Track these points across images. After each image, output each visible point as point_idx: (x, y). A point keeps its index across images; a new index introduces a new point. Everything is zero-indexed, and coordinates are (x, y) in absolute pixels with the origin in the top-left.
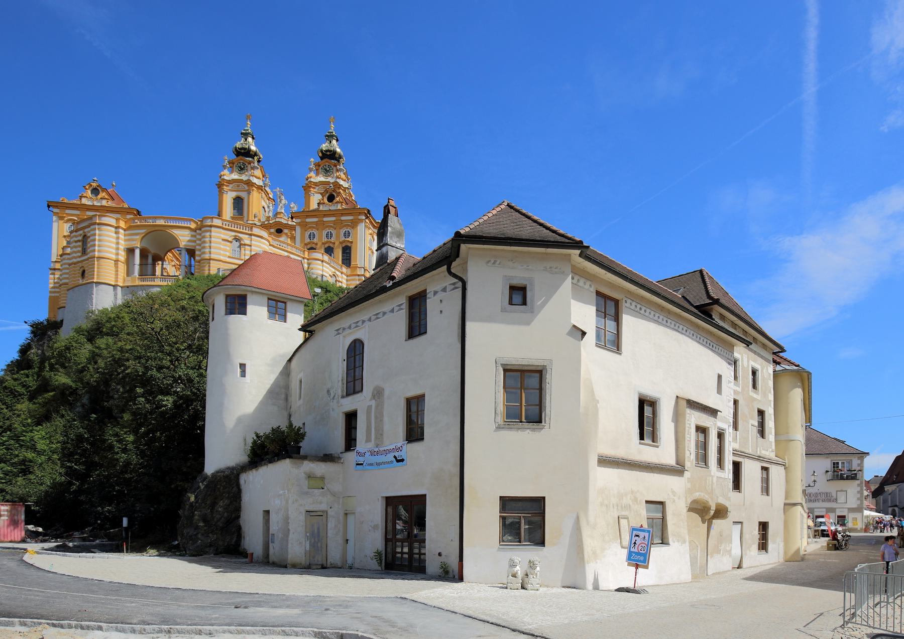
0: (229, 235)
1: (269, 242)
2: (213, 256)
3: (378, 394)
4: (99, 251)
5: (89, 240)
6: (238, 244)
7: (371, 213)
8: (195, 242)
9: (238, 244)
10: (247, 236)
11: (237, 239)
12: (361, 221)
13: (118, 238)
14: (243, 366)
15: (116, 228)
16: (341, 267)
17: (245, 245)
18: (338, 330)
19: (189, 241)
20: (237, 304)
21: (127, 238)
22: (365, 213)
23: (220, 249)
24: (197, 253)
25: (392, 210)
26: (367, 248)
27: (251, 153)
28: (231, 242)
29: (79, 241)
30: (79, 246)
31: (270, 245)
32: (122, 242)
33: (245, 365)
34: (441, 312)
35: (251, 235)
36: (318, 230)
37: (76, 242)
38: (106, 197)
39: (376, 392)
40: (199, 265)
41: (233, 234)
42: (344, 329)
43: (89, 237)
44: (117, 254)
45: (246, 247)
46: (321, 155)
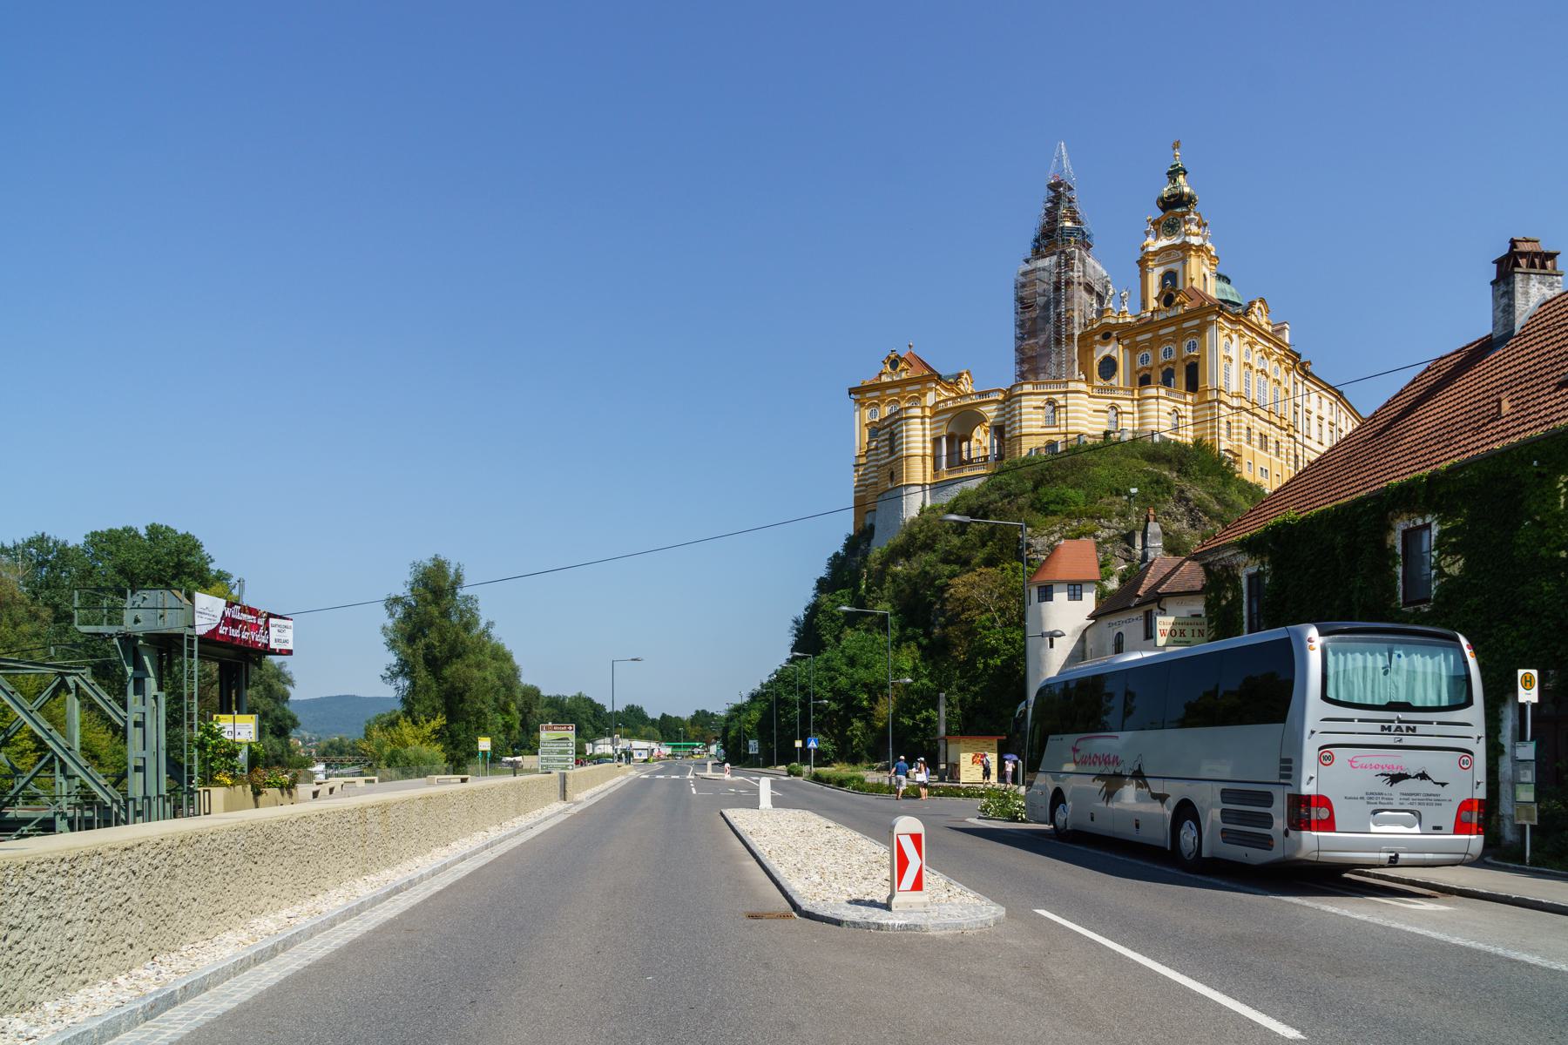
0: (1040, 401)
2: (1024, 431)
4: (907, 449)
6: (1051, 407)
8: (1004, 415)
9: (1051, 407)
11: (1050, 402)
12: (1211, 323)
13: (924, 429)
15: (923, 417)
17: (1060, 407)
19: (997, 416)
20: (1046, 594)
21: (933, 426)
23: (1031, 420)
24: (1007, 429)
28: (1043, 408)
29: (886, 439)
32: (928, 432)
35: (1066, 393)
44: (924, 448)
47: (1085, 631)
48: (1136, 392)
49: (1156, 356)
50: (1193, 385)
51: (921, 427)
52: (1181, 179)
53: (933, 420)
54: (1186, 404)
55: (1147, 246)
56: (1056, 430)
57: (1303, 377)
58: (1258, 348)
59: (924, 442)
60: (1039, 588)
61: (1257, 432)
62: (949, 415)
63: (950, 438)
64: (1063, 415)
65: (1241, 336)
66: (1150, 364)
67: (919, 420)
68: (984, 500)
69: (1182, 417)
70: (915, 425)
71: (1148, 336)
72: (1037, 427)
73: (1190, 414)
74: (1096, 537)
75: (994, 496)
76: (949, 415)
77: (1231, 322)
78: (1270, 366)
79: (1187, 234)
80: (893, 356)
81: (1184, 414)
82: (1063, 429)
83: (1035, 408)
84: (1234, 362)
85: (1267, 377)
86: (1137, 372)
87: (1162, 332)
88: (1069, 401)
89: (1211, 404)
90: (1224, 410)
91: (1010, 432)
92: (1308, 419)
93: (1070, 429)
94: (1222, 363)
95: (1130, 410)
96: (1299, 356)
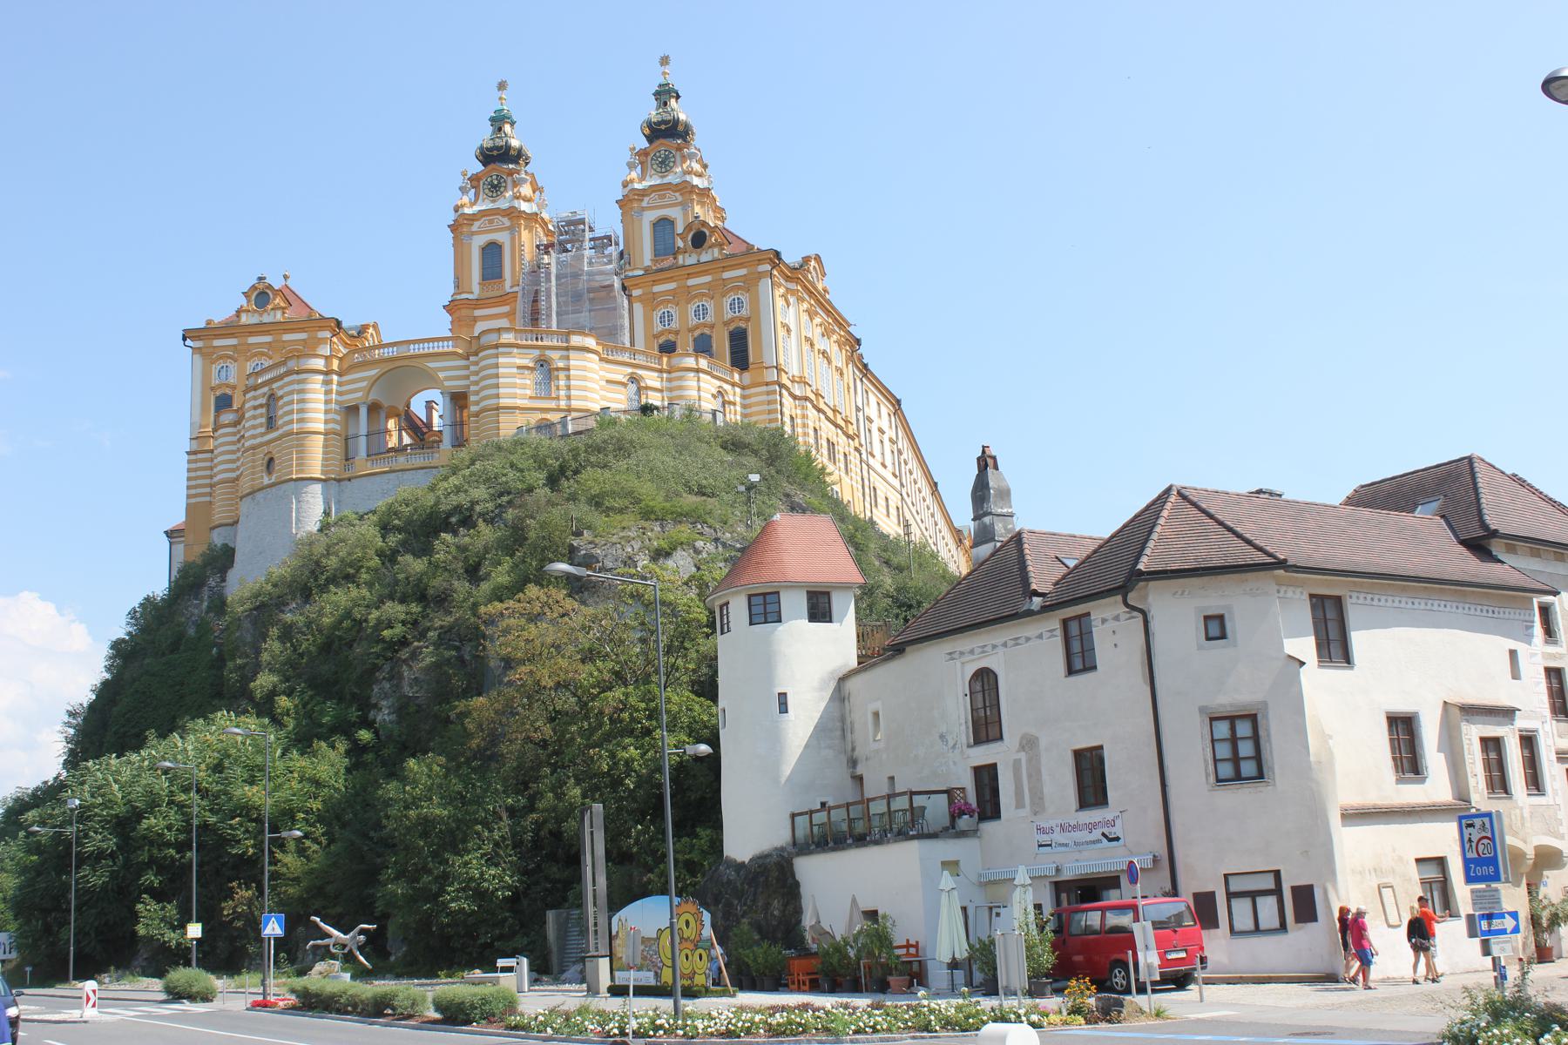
2: (503, 402)
3: (1029, 744)
5: (281, 403)
7: (870, 367)
8: (467, 377)
14: (783, 698)
15: (327, 373)
16: (732, 372)
17: (558, 369)
18: (950, 654)
20: (766, 609)
22: (770, 259)
23: (514, 386)
24: (473, 398)
25: (990, 461)
26: (779, 325)
27: (512, 152)
29: (261, 406)
30: (261, 415)
33: (785, 694)
34: (1115, 645)
35: (567, 349)
36: (677, 305)
37: (255, 408)
38: (282, 304)
39: (1024, 742)
40: (477, 422)
42: (962, 653)
43: (282, 397)
46: (647, 131)
47: (843, 679)
48: (665, 359)
49: (684, 316)
50: (740, 359)
54: (733, 385)
56: (552, 405)
57: (861, 371)
58: (818, 320)
60: (750, 597)
61: (824, 436)
62: (373, 372)
63: (374, 408)
65: (800, 300)
66: (674, 325)
68: (462, 499)
69: (730, 403)
70: (316, 384)
71: (672, 286)
72: (523, 397)
73: (738, 399)
74: (697, 552)
75: (480, 493)
76: (373, 372)
77: (788, 279)
78: (834, 350)
81: (732, 399)
82: (563, 404)
84: (793, 334)
85: (829, 362)
86: (656, 337)
87: (691, 282)
89: (771, 388)
90: (787, 400)
91: (477, 403)
92: (869, 431)
93: (575, 404)
94: (781, 333)
95: (657, 384)
96: (858, 342)
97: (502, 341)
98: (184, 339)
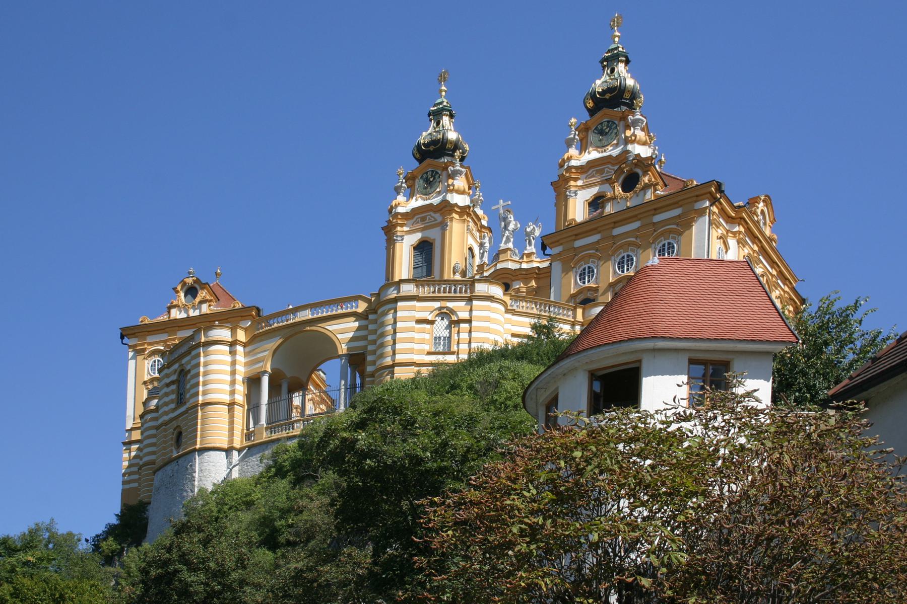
0: (426, 309)
1: (504, 303)
2: (399, 358)
5: (189, 377)
8: (365, 338)
9: (446, 322)
10: (463, 304)
13: (234, 363)
17: (459, 322)
19: (352, 339)
23: (411, 340)
24: (370, 358)
28: (432, 322)
29: (173, 383)
30: (172, 392)
31: (507, 311)
41: (437, 304)
43: (189, 371)
44: (233, 392)
45: (462, 325)
51: (229, 358)
52: (621, 68)
53: (248, 349)
55: (569, 159)
59: (233, 383)
64: (464, 336)
67: (227, 348)
72: (420, 352)
79: (627, 141)
80: (190, 281)
83: (419, 321)
88: (474, 313)
97: (402, 294)
98: (122, 337)
